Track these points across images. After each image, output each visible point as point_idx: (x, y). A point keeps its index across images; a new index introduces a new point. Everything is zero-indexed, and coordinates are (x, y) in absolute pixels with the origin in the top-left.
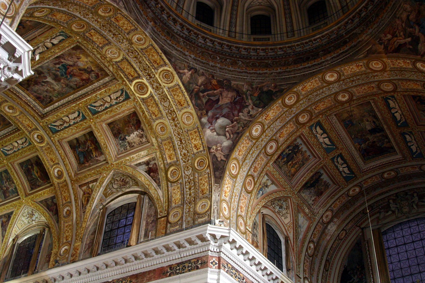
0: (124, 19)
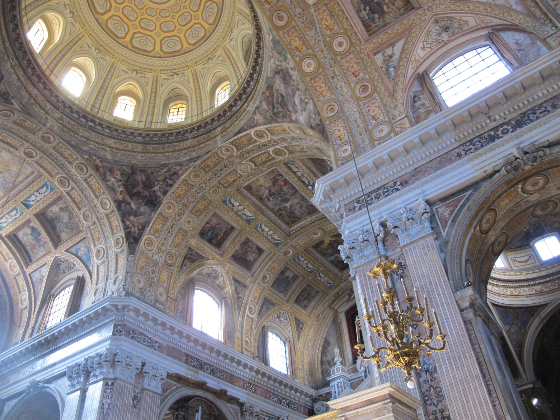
0: (206, 161)
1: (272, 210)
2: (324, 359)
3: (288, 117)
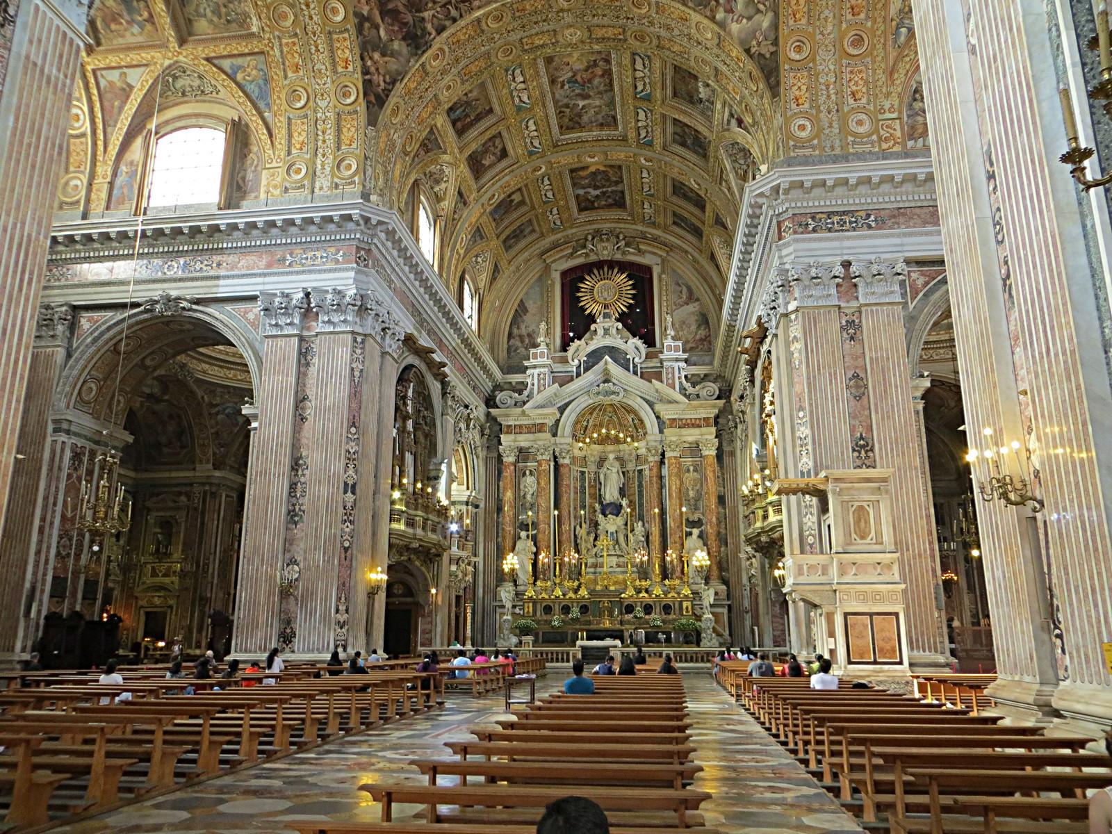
1: (556, 102)
2: (515, 331)
3: (709, 8)
